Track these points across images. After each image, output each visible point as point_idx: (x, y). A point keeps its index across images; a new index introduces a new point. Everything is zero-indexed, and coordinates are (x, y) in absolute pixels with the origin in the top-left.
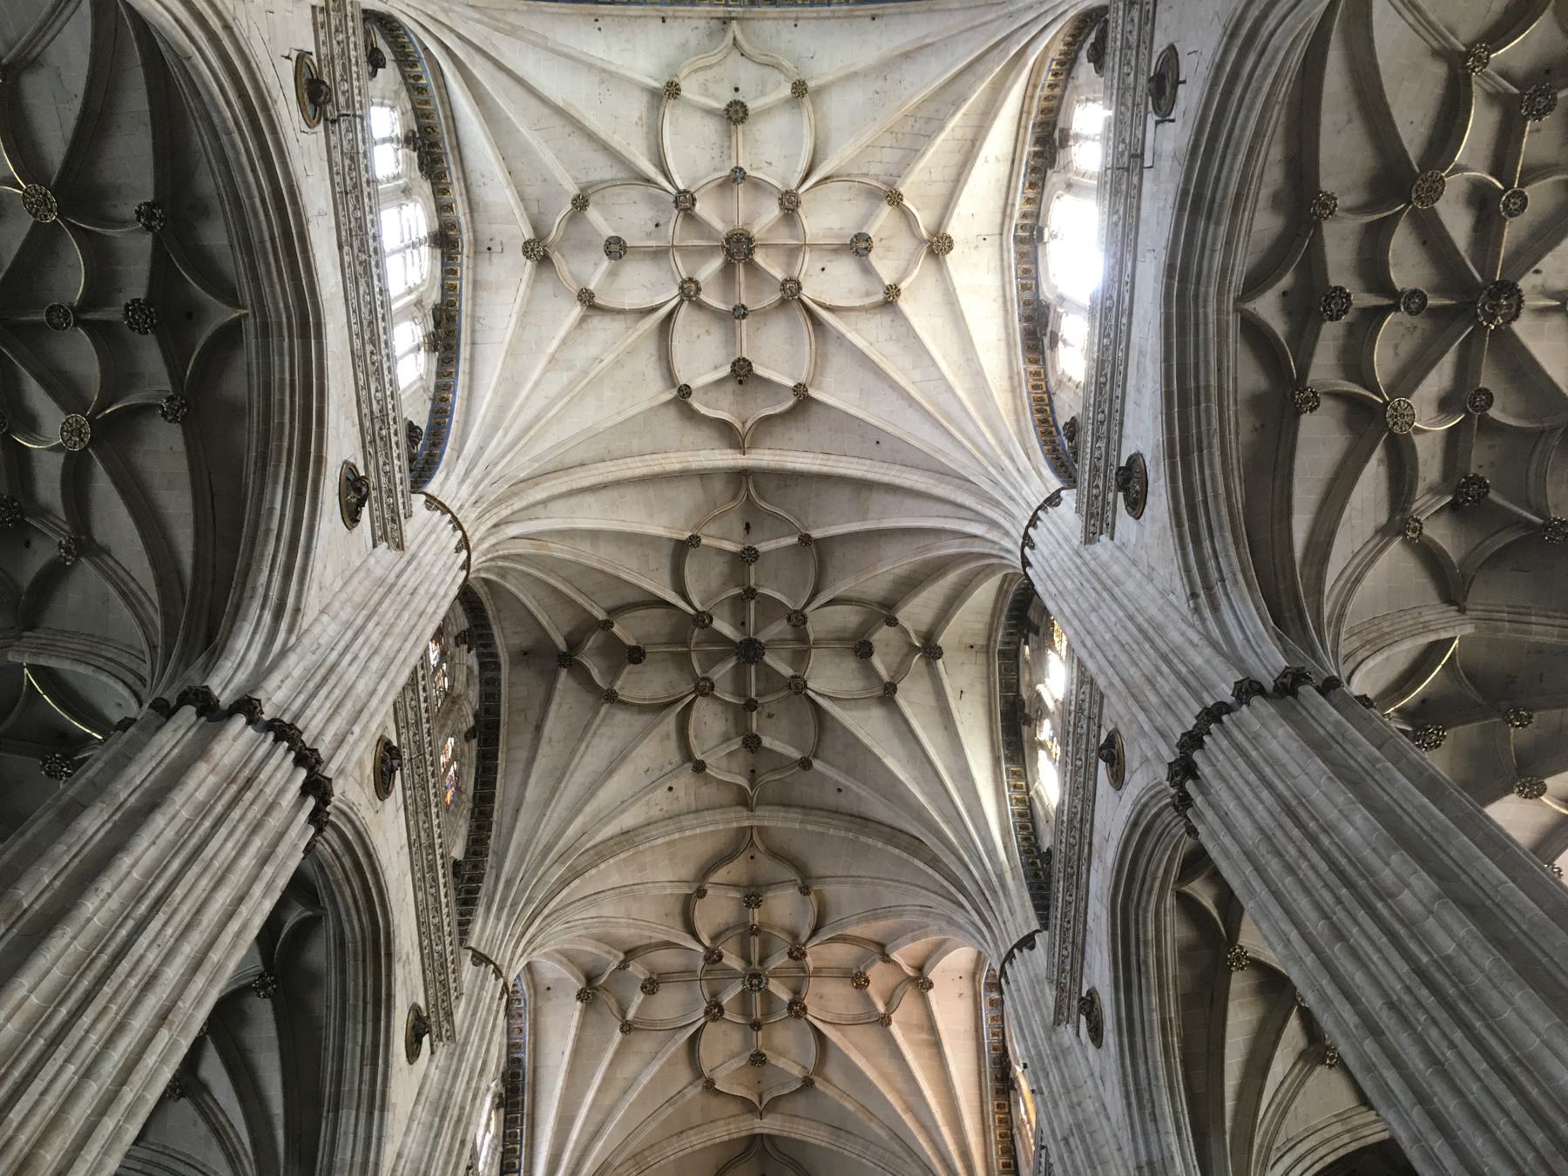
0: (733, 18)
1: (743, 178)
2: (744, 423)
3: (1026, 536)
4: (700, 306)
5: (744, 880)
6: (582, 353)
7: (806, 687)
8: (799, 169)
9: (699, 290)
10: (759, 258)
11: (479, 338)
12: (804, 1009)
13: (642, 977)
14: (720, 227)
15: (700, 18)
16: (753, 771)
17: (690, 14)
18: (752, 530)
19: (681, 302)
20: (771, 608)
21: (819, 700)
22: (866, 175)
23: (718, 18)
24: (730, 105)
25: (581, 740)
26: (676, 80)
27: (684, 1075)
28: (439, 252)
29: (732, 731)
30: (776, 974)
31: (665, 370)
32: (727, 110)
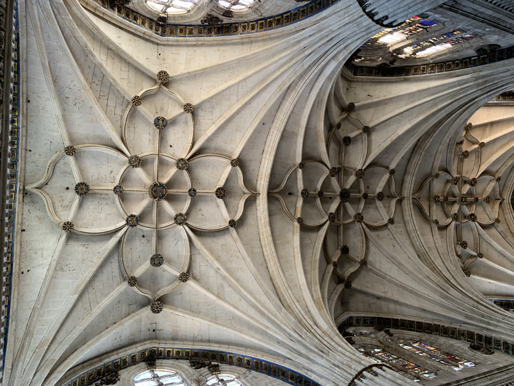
0: (24, 188)
1: (120, 187)
2: (244, 193)
3: (378, 22)
4: (188, 213)
5: (427, 203)
6: (214, 280)
7: (361, 170)
8: (116, 155)
9: (181, 215)
10: (165, 181)
11: (206, 337)
12: (474, 179)
13: (461, 248)
14: (146, 201)
15: (23, 208)
16: (388, 196)
17: (20, 214)
18: (292, 191)
19: (187, 224)
20: (326, 184)
21: (367, 164)
22: (122, 117)
23: (23, 197)
24: (78, 193)
25: (384, 278)
26: (62, 224)
27: (493, 231)
28: (158, 362)
29: (374, 206)
30: (460, 190)
31: (220, 233)
32: (81, 194)
